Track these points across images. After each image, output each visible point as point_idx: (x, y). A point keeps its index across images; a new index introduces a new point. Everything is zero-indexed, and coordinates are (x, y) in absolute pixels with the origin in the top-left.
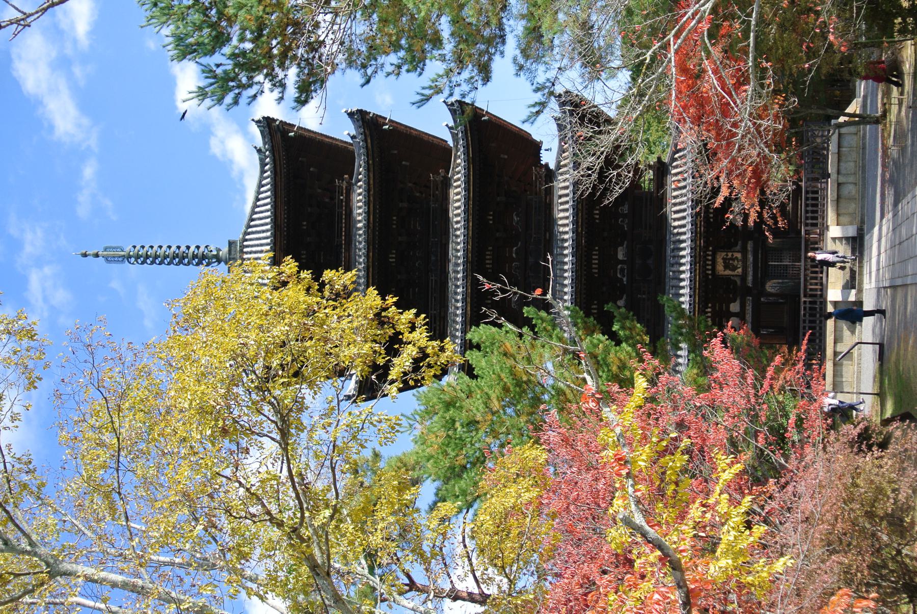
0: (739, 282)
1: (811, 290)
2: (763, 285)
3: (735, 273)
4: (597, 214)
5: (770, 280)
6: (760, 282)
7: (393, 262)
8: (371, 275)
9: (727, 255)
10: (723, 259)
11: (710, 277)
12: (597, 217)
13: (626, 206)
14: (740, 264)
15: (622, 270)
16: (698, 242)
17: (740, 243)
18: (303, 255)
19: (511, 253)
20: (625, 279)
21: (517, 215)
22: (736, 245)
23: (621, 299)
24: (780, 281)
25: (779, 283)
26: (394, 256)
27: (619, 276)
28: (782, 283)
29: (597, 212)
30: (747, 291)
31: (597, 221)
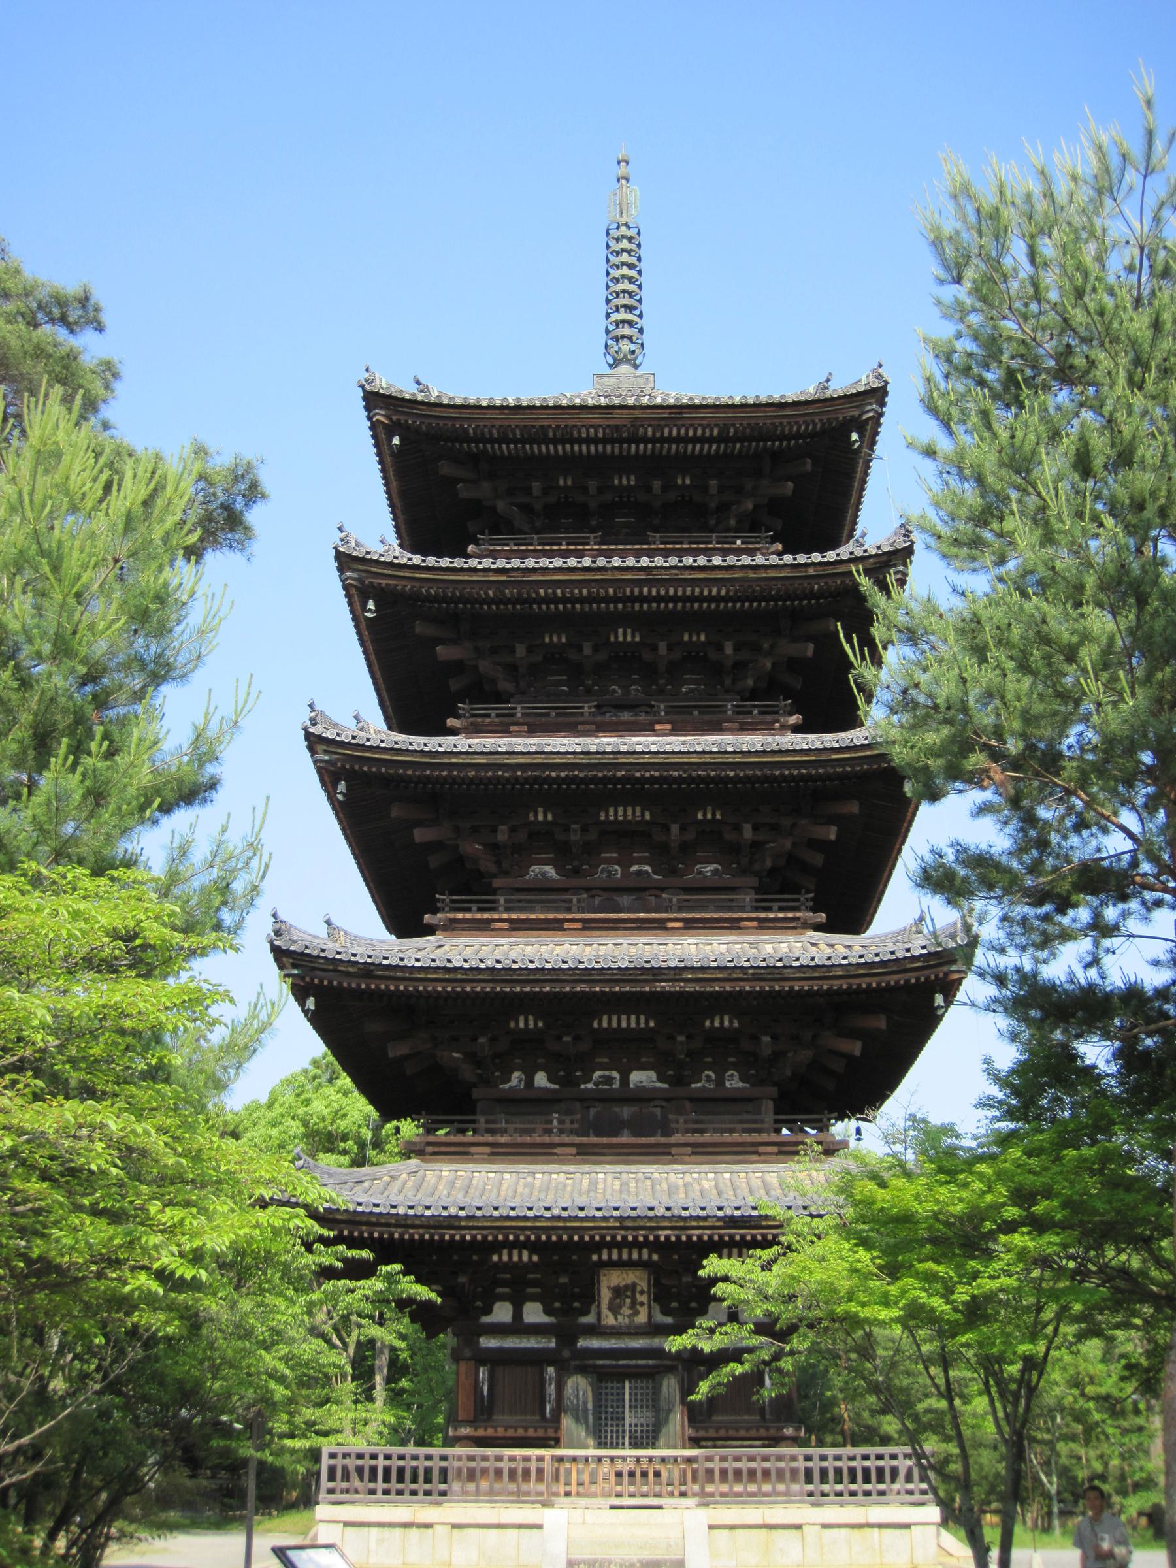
0: (585, 1320)
1: (569, 1472)
2: (583, 1370)
3: (605, 1311)
4: (722, 1022)
5: (591, 1385)
6: (585, 1363)
7: (616, 637)
8: (588, 577)
9: (642, 1292)
10: (634, 1285)
12: (717, 1024)
13: (740, 1085)
14: (623, 1320)
15: (609, 1079)
17: (669, 1320)
18: (628, 480)
19: (640, 861)
20: (590, 1086)
21: (715, 872)
22: (665, 1312)
23: (550, 1080)
24: (590, 1406)
25: (585, 1403)
26: (629, 639)
27: (597, 1074)
28: (586, 1410)
29: (726, 1023)
30: (567, 1333)
31: (707, 1023)
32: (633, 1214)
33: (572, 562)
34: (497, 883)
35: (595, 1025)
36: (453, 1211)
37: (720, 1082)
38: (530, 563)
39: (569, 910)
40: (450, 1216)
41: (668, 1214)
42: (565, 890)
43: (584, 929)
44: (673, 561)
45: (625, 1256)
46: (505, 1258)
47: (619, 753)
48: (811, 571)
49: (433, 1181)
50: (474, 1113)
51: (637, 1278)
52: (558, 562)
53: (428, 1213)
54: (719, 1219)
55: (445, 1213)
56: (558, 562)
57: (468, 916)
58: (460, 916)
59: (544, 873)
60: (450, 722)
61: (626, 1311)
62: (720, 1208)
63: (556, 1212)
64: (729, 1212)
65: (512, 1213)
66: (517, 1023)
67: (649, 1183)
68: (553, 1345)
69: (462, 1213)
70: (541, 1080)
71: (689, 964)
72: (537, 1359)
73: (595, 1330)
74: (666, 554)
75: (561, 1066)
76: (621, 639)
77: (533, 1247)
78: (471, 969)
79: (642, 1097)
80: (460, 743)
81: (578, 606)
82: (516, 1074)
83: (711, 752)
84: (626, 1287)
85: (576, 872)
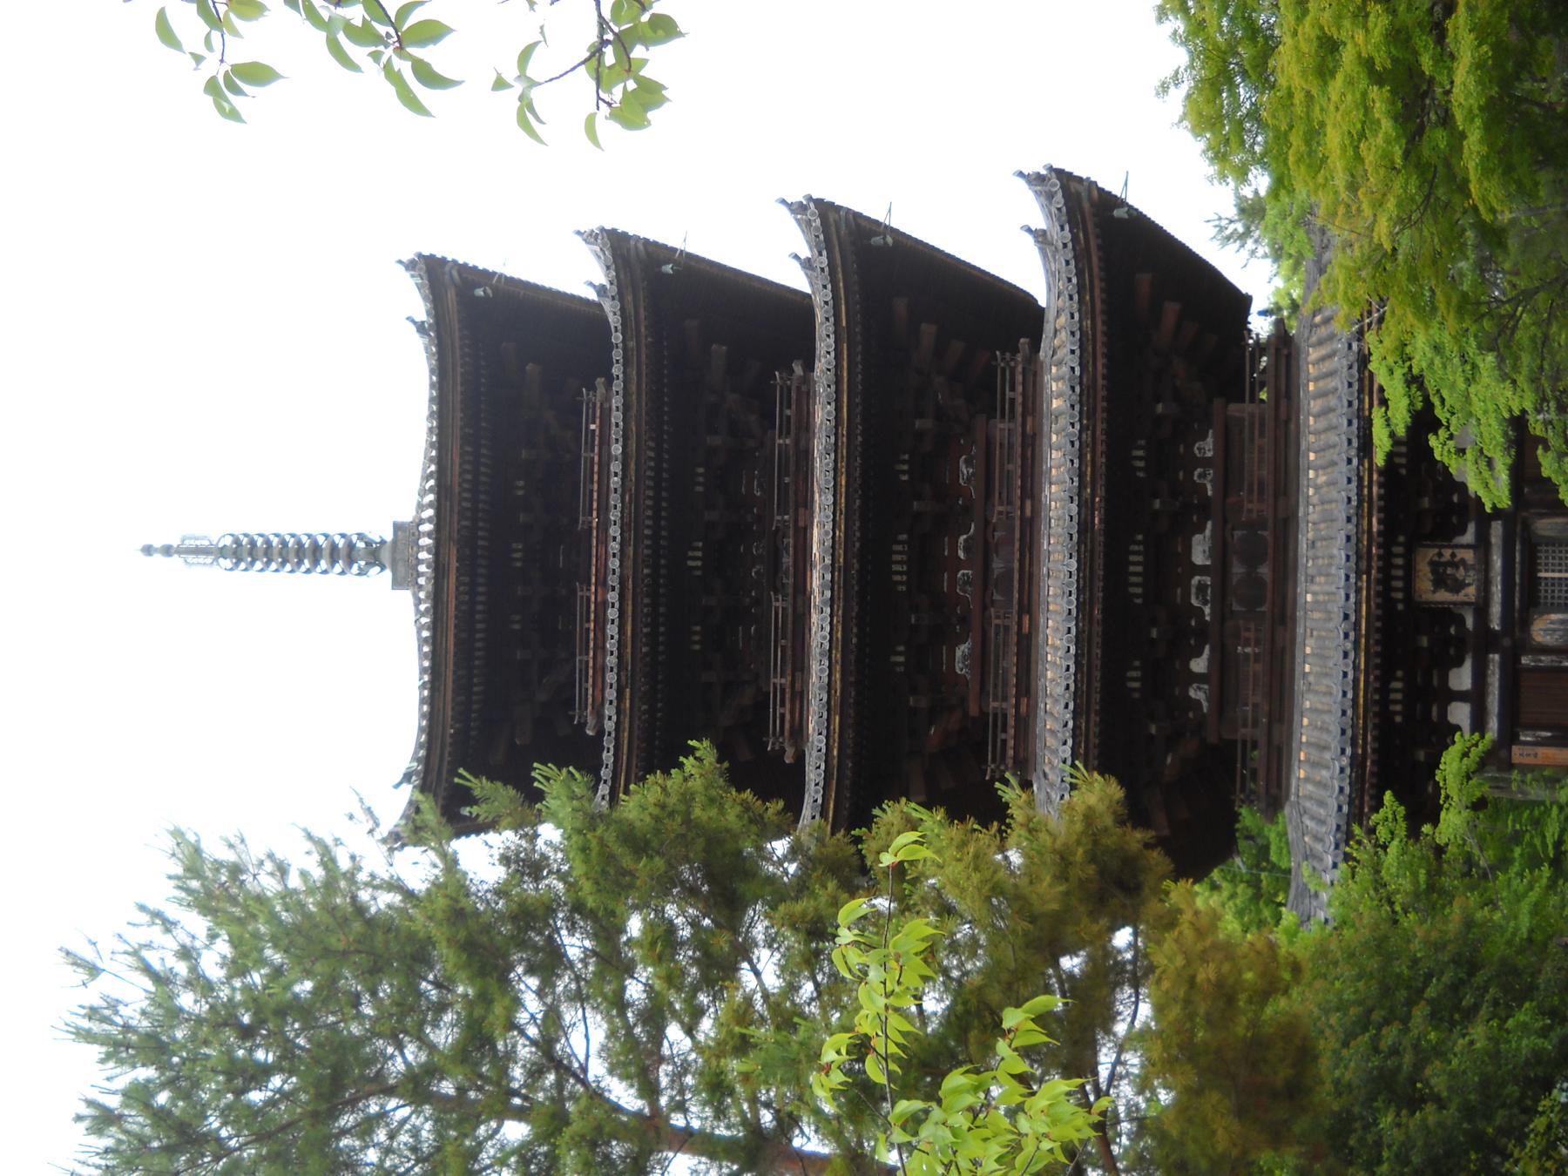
0: (1470, 622)
2: (1526, 624)
3: (1460, 597)
4: (1140, 458)
5: (1542, 614)
7: (696, 568)
8: (630, 596)
9: (1440, 555)
11: (1400, 607)
13: (1210, 440)
15: (1201, 588)
16: (1365, 522)
17: (1471, 528)
20: (1207, 610)
21: (968, 463)
22: (1463, 532)
23: (1199, 654)
26: (699, 554)
27: (1194, 602)
29: (1140, 453)
30: (1485, 641)
32: (1353, 558)
33: (612, 613)
34: (973, 710)
35: (1139, 601)
36: (1345, 761)
37: (1206, 463)
38: (611, 661)
39: (1007, 629)
40: (1351, 765)
41: (1354, 520)
42: (984, 634)
43: (1029, 612)
44: (614, 499)
45: (1400, 573)
46: (1398, 708)
47: (833, 565)
48: (632, 344)
49: (1310, 787)
50: (1236, 741)
51: (1425, 558)
52: (612, 630)
53: (1347, 790)
54: (1361, 463)
55: (1348, 771)
56: (612, 630)
57: (1011, 743)
58: (1011, 753)
59: (964, 656)
60: (788, 760)
61: (1461, 573)
62: (1349, 461)
63: (1349, 646)
64: (1353, 452)
65: (1350, 695)
66: (1135, 690)
67: (1319, 544)
68: (1497, 657)
69: (1349, 751)
70: (1199, 665)
71: (1076, 491)
72: (1513, 678)
73: (1482, 609)
74: (604, 509)
75: (1186, 636)
76: (699, 563)
77: (1386, 677)
78: (1074, 737)
79: (1221, 551)
80: (816, 739)
81: (662, 610)
82: (1192, 693)
83: (836, 461)
84: (1434, 572)
85: (963, 620)
